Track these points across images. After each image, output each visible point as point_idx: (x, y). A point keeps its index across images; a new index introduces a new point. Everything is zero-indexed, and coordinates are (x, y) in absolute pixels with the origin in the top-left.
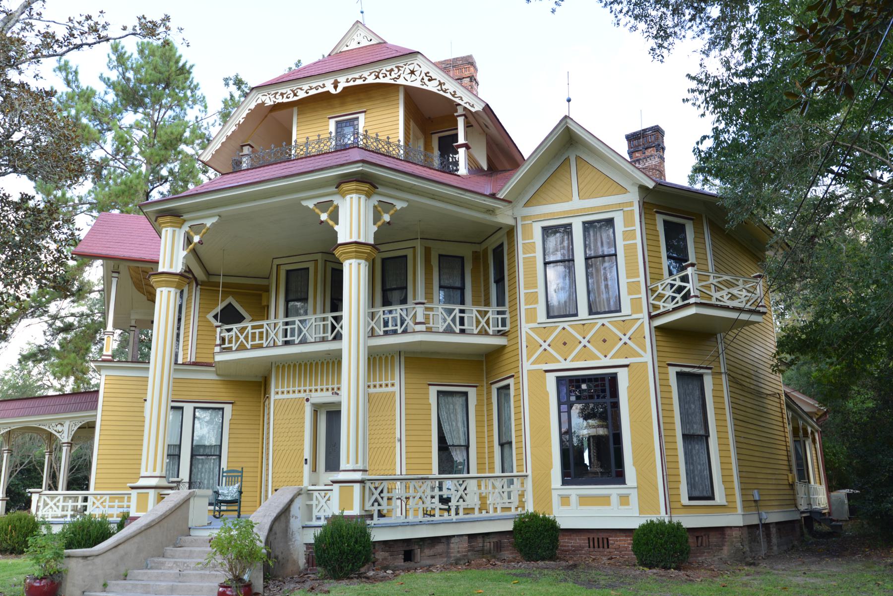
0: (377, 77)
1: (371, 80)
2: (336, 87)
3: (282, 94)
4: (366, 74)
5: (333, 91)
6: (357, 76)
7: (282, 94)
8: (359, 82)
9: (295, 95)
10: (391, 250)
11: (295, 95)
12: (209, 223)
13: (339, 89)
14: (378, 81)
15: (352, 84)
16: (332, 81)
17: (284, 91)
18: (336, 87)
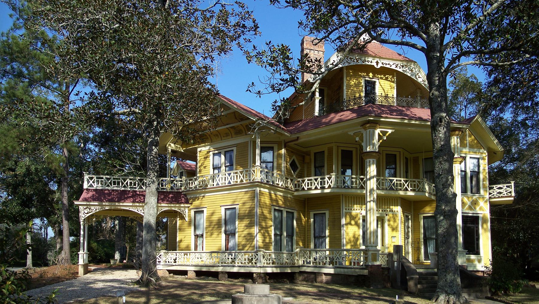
0: (396, 67)
1: (393, 67)
2: (377, 65)
3: (351, 59)
4: (391, 63)
5: (376, 66)
6: (387, 63)
7: (351, 59)
8: (388, 66)
9: (357, 61)
10: (392, 151)
11: (357, 61)
12: (390, 131)
13: (379, 67)
14: (396, 69)
15: (385, 66)
16: (376, 61)
17: (351, 57)
18: (377, 65)
